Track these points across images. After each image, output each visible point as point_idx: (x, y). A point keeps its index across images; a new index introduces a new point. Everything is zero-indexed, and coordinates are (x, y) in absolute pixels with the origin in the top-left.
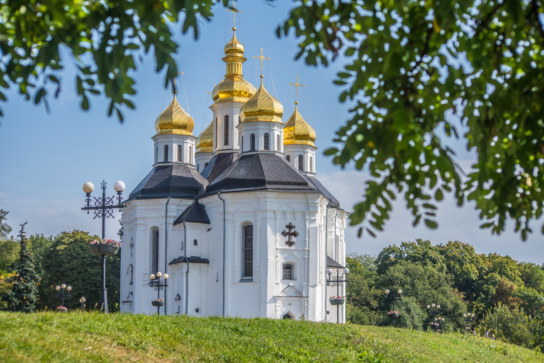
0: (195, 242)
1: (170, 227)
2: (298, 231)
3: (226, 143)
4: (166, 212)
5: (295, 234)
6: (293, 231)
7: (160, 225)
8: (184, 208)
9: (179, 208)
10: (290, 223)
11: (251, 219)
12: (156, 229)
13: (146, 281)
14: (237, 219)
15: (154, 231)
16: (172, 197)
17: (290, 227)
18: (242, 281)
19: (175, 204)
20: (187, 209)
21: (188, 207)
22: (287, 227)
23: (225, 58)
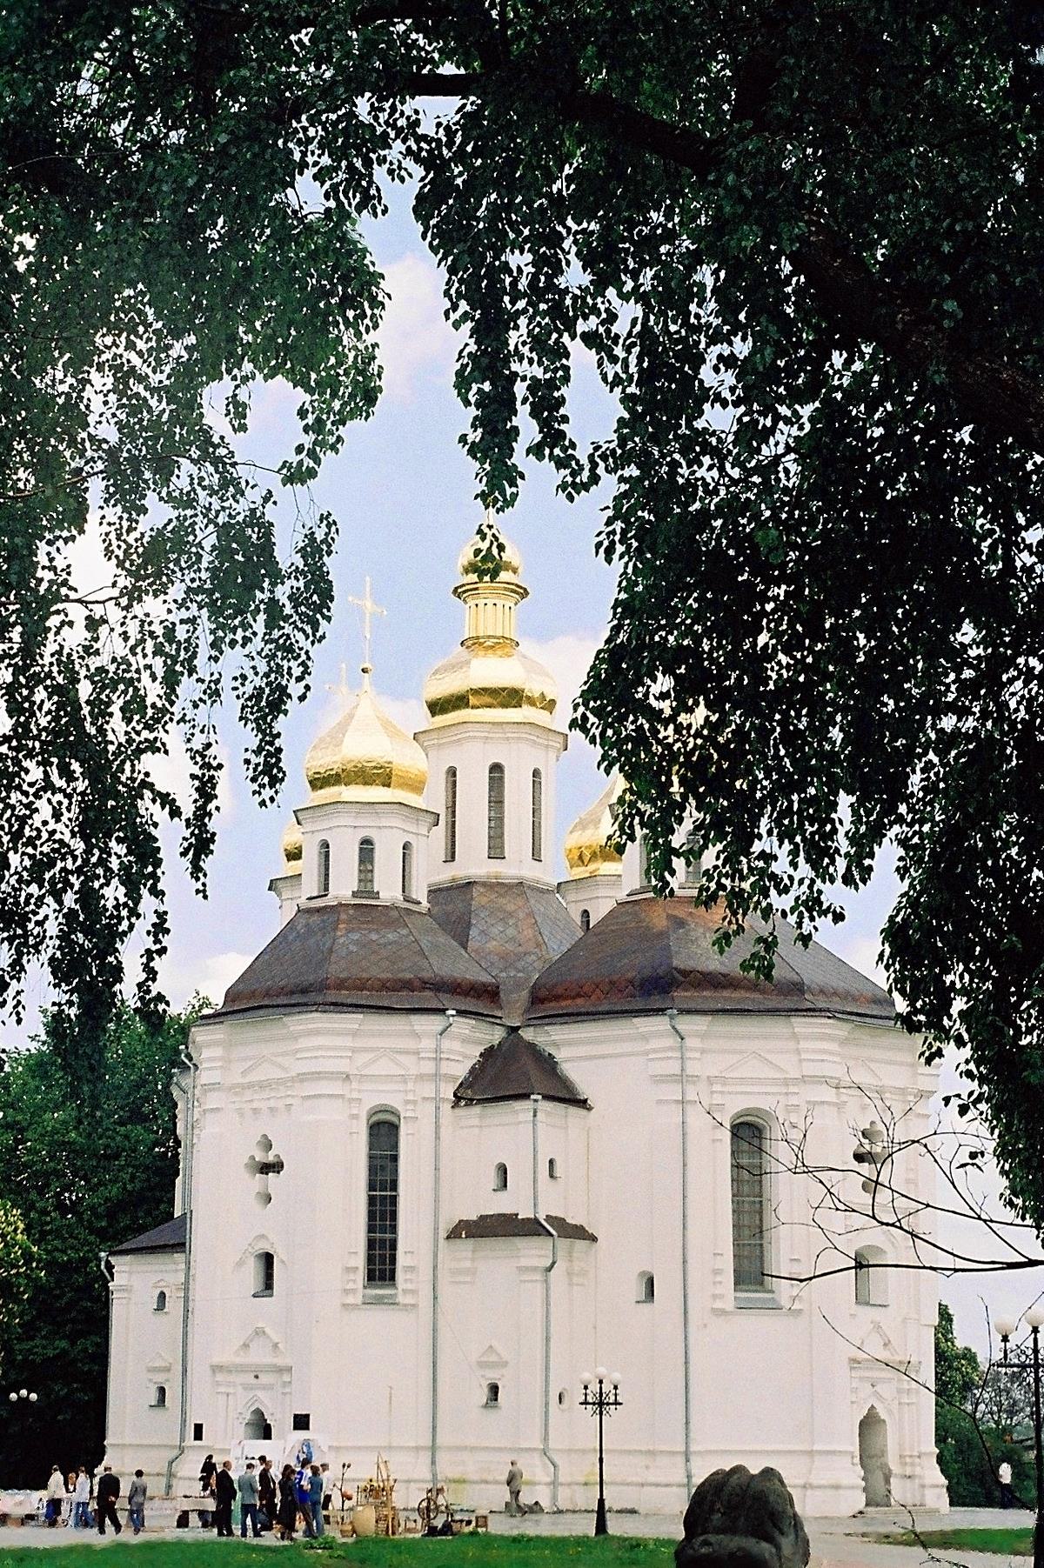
3: (496, 849)
7: (407, 1102)
12: (394, 1119)
14: (717, 1099)
15: (375, 1119)
16: (461, 1013)
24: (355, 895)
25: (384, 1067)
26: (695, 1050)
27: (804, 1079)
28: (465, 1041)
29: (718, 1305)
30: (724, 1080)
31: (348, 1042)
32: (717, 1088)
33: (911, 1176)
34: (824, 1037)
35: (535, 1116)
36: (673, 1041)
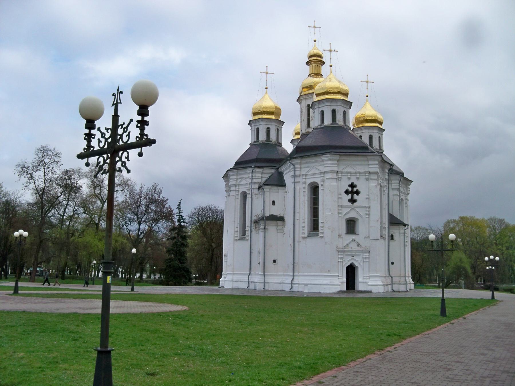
0: (274, 203)
1: (256, 191)
2: (359, 190)
4: (252, 179)
5: (358, 193)
6: (355, 189)
7: (247, 190)
8: (268, 176)
9: (264, 175)
10: (353, 183)
11: (318, 180)
13: (237, 236)
14: (304, 180)
16: (256, 167)
17: (352, 186)
18: (309, 236)
19: (259, 173)
20: (270, 177)
21: (270, 175)
22: (350, 186)
23: (308, 62)
24: (254, 142)
25: (244, 182)
26: (298, 168)
27: (324, 173)
28: (262, 173)
29: (303, 236)
30: (306, 175)
31: (235, 177)
32: (304, 177)
33: (367, 197)
34: (330, 160)
35: (264, 190)
36: (292, 167)
